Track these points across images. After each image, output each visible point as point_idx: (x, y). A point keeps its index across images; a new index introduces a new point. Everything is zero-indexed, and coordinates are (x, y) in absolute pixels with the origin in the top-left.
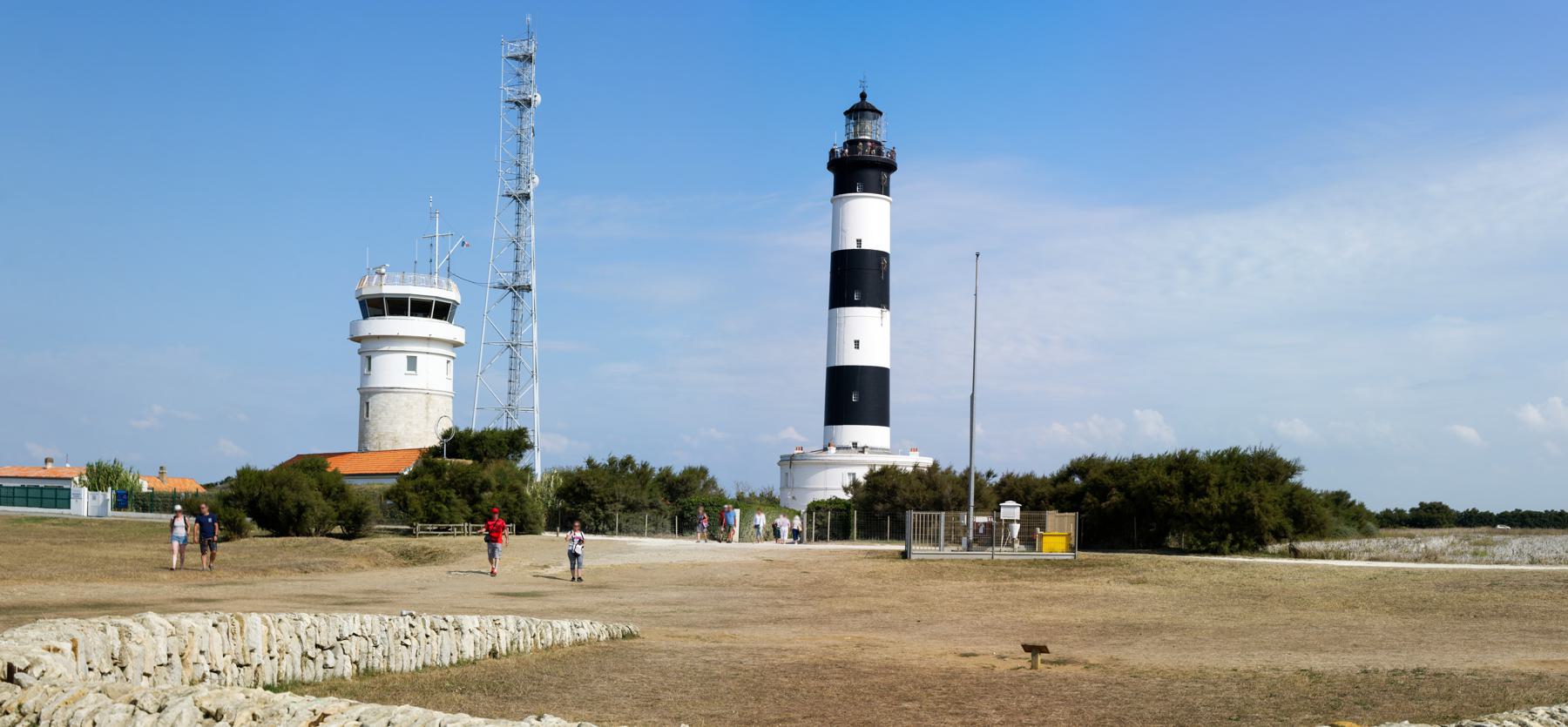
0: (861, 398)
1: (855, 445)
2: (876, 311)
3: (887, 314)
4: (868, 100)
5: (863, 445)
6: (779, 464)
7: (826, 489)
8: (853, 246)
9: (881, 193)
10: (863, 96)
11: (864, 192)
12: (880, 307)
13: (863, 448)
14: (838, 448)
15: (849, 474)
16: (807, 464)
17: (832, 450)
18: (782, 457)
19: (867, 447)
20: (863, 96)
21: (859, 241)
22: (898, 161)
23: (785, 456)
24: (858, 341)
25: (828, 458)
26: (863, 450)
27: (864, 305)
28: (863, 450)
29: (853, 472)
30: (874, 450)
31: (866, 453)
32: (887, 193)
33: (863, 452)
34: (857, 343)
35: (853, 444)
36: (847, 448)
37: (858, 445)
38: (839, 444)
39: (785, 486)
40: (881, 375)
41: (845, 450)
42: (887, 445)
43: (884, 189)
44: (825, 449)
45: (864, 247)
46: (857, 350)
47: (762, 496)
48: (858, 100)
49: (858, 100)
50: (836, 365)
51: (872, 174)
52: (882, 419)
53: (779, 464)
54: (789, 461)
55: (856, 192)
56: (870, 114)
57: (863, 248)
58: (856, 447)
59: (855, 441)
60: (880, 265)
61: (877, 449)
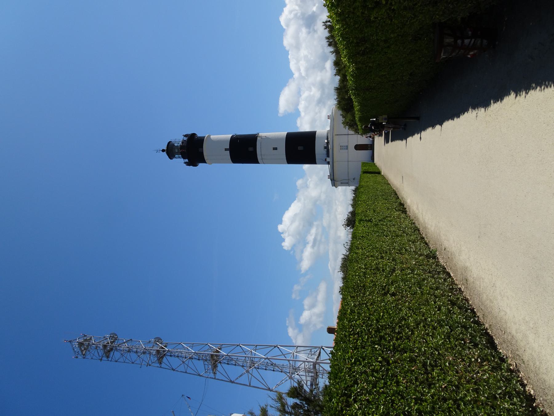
1: (325, 148)
6: (336, 187)
10: (163, 151)
18: (333, 186)
20: (163, 151)
21: (226, 150)
22: (190, 132)
35: (325, 149)
37: (326, 146)
38: (325, 156)
45: (228, 147)
47: (354, 194)
48: (165, 154)
49: (165, 152)
53: (336, 187)
57: (228, 148)
58: (327, 147)
59: (323, 148)
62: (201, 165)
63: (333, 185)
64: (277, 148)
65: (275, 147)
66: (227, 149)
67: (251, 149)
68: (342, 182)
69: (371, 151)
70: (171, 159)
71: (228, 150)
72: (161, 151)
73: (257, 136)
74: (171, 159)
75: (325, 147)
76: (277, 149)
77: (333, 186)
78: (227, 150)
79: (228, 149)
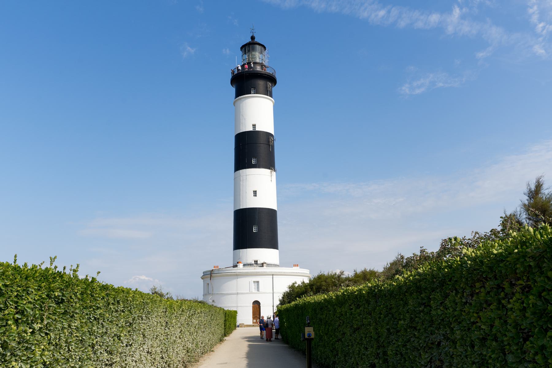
0: (259, 229)
1: (256, 262)
2: (267, 171)
3: (274, 173)
4: (256, 40)
5: (262, 262)
6: (202, 278)
7: (238, 294)
8: (250, 129)
9: (268, 96)
10: (253, 38)
11: (256, 94)
12: (269, 169)
13: (263, 264)
14: (244, 265)
15: (254, 282)
16: (223, 276)
17: (241, 266)
19: (265, 263)
20: (253, 38)
21: (254, 126)
23: (206, 272)
24: (256, 192)
25: (238, 271)
26: (262, 265)
27: (259, 167)
28: (262, 265)
29: (257, 280)
30: (269, 265)
31: (265, 267)
32: (271, 96)
33: (263, 266)
34: (255, 193)
36: (251, 265)
37: (259, 262)
38: (245, 262)
39: (207, 293)
40: (271, 214)
41: (249, 266)
42: (277, 263)
43: (268, 93)
44: (235, 266)
45: (257, 129)
46: (255, 197)
48: (249, 40)
49: (250, 40)
50: (241, 208)
51: (261, 83)
52: (273, 245)
53: (202, 278)
54: (209, 275)
55: (251, 94)
56: (258, 47)
57: (257, 130)
58: (257, 264)
59: (256, 259)
60: (269, 142)
61: (271, 265)
62: (233, 90)
63: (205, 274)
64: (256, 196)
65: (257, 192)
66: (255, 127)
67: (253, 162)
68: (210, 284)
69: (251, 323)
70: (242, 48)
71: (253, 129)
72: (251, 35)
73: (272, 170)
74: (241, 48)
75: (257, 261)
76: (254, 196)
77: (204, 273)
78: (253, 127)
79: (255, 129)
